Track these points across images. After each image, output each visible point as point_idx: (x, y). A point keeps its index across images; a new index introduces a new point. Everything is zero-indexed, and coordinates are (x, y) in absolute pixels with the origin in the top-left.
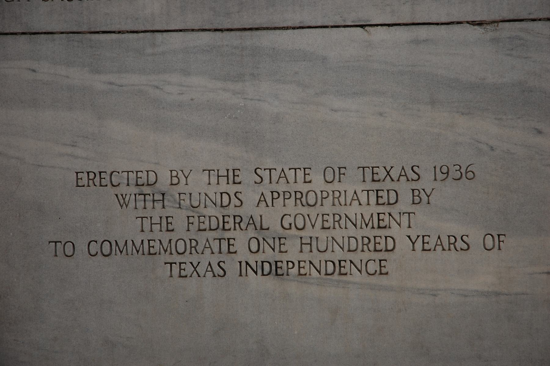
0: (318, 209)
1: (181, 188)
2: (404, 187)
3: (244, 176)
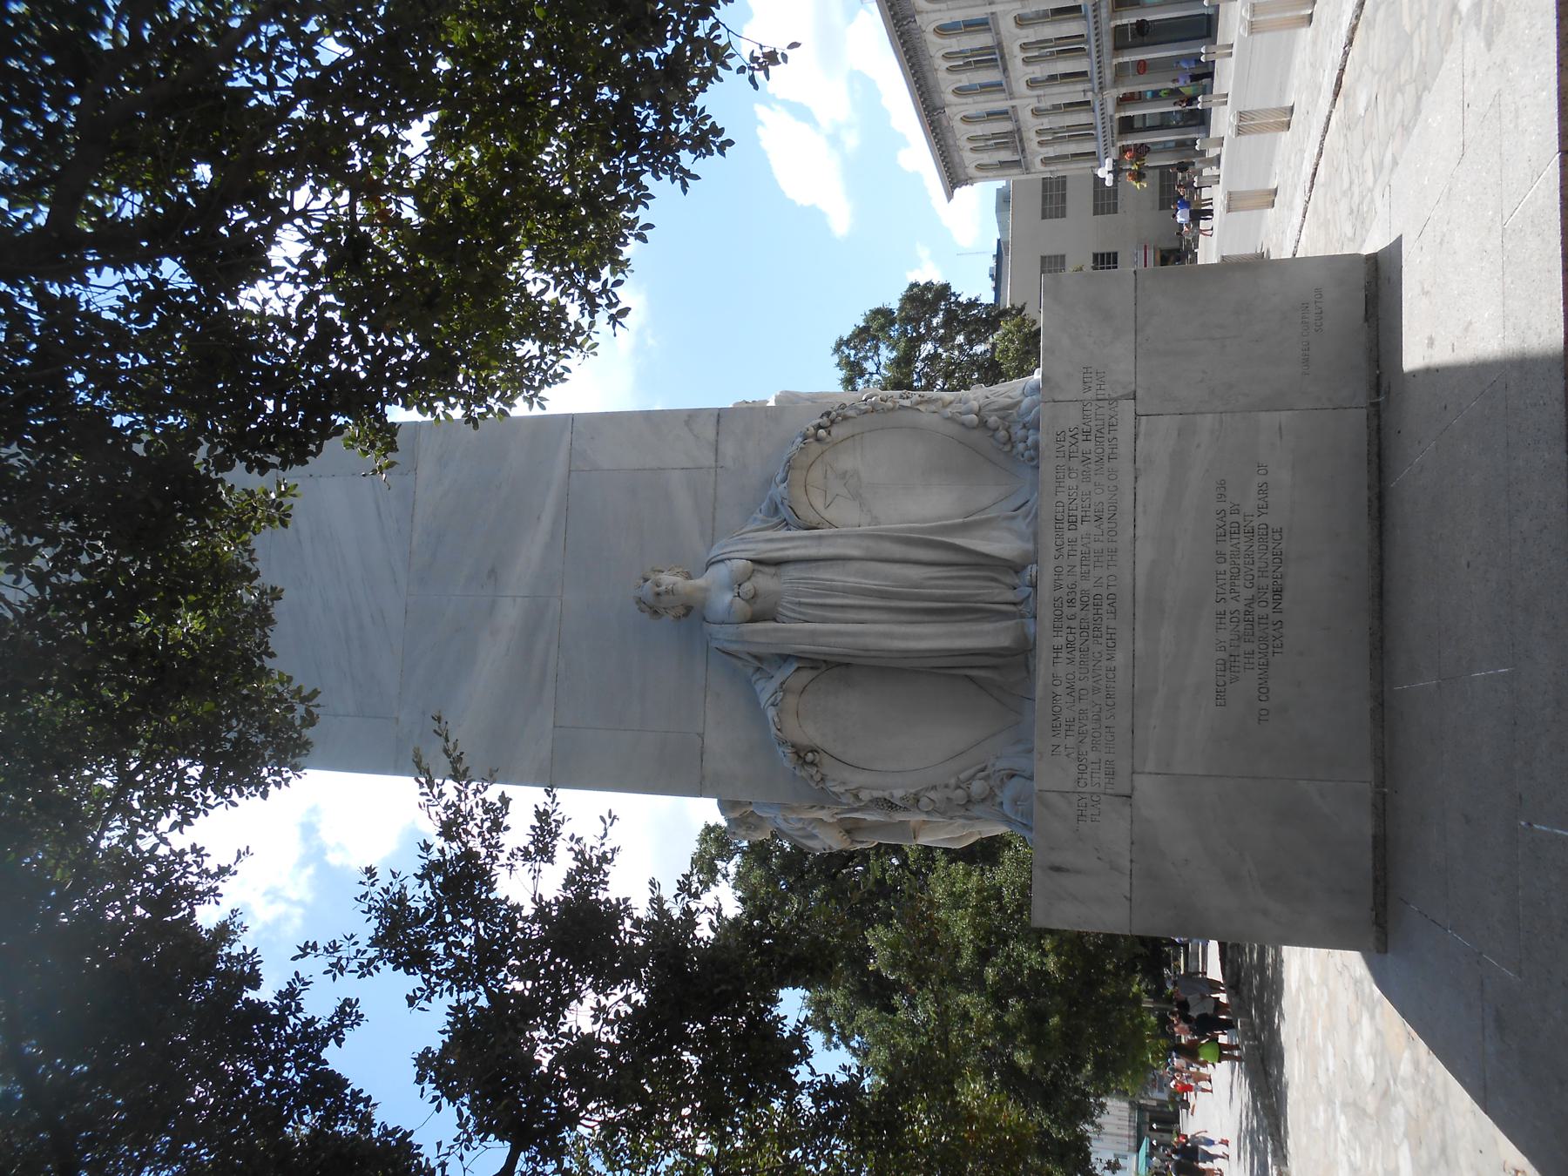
0: (1241, 567)
1: (1227, 646)
2: (1230, 518)
3: (1221, 607)
